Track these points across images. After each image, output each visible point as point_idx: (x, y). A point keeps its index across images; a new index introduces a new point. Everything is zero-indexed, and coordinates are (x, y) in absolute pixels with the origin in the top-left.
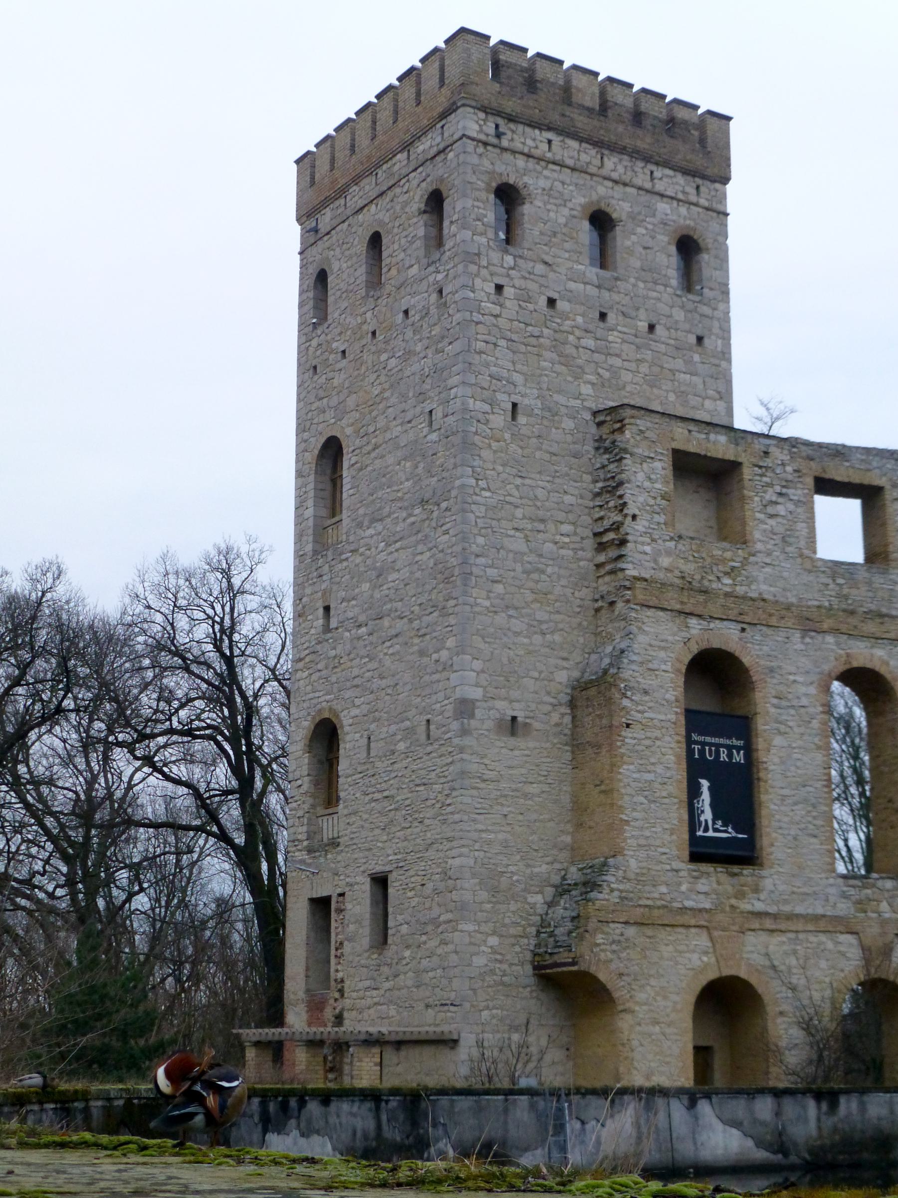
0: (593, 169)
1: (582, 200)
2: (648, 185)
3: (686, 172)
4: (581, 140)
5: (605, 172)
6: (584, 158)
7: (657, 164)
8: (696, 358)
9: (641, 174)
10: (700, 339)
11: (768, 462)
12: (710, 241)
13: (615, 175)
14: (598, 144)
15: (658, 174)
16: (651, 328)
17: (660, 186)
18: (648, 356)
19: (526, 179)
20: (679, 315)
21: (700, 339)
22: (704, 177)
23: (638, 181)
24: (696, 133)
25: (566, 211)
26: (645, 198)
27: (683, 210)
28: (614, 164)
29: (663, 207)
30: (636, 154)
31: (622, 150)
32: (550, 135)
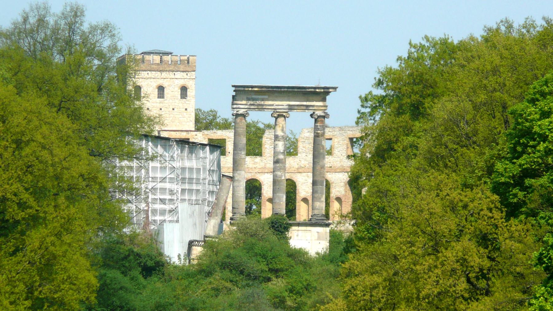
0: (158, 77)
1: (156, 85)
2: (173, 77)
3: (183, 72)
4: (155, 71)
5: (162, 77)
6: (157, 75)
7: (176, 71)
8: (185, 114)
9: (171, 75)
10: (186, 109)
11: (196, 137)
12: (189, 86)
13: (165, 77)
14: (160, 71)
15: (176, 73)
16: (173, 109)
17: (176, 77)
18: (172, 116)
19: (142, 83)
20: (181, 105)
21: (186, 109)
22: (188, 72)
23: (170, 77)
24: (186, 62)
25: (152, 88)
26: (172, 80)
27: (183, 80)
28: (164, 74)
29: (176, 81)
30: (169, 71)
31: (167, 71)
32: (148, 72)
